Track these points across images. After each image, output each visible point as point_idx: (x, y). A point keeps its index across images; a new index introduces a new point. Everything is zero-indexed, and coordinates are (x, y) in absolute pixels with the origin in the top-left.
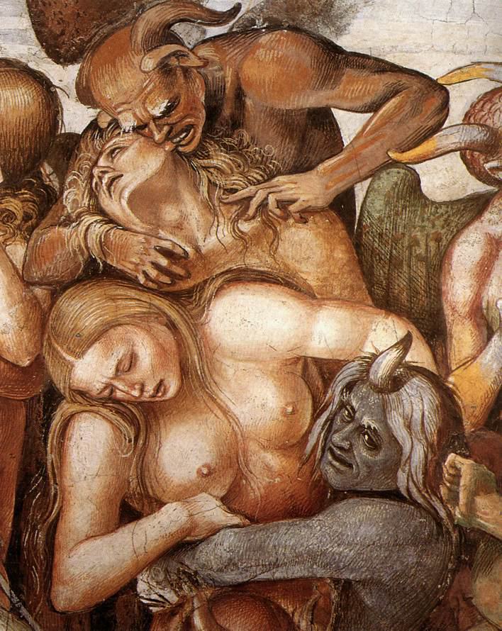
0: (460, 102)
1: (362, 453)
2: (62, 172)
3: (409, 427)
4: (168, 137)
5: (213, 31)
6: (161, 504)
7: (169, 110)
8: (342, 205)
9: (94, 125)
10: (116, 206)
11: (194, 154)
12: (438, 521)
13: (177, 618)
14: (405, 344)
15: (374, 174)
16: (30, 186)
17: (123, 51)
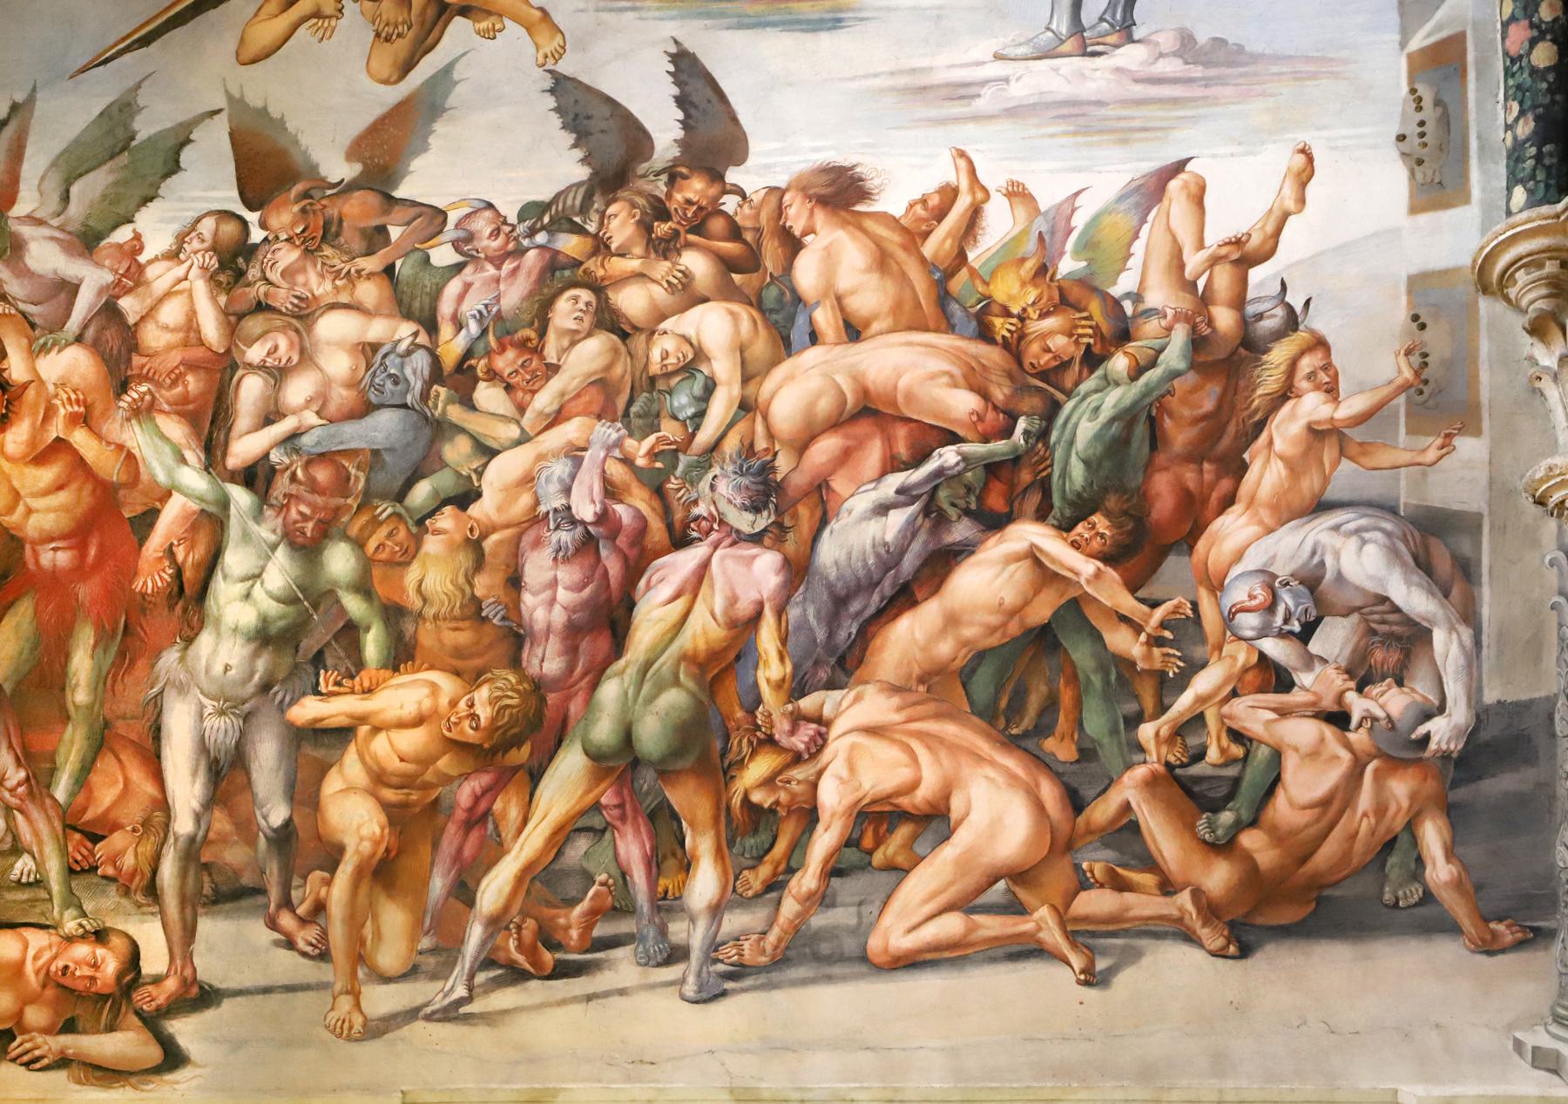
0: (453, 217)
1: (389, 385)
2: (247, 261)
3: (414, 373)
4: (303, 243)
5: (329, 192)
6: (285, 416)
7: (303, 231)
8: (389, 270)
9: (266, 239)
10: (274, 276)
11: (315, 250)
12: (426, 418)
13: (289, 472)
14: (416, 334)
15: (406, 255)
16: (231, 268)
17: (286, 203)
